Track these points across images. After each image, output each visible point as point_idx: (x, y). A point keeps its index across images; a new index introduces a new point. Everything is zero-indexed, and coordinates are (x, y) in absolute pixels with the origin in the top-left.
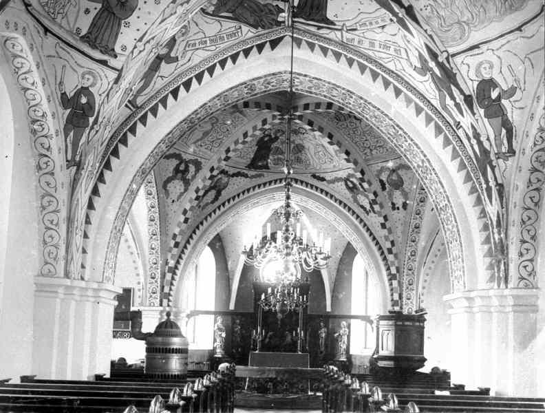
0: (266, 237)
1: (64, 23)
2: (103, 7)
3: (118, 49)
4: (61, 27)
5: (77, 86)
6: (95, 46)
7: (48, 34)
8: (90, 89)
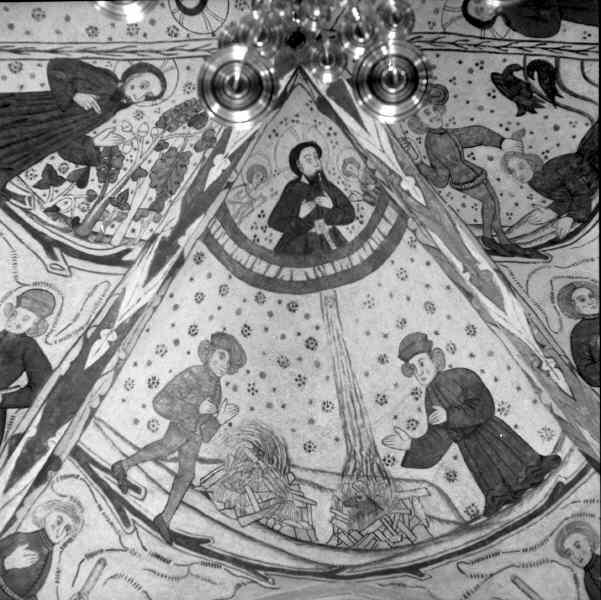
1: (437, 529)
2: (456, 441)
3: (543, 448)
4: (435, 540)
5: (575, 578)
6: (516, 493)
7: (422, 570)
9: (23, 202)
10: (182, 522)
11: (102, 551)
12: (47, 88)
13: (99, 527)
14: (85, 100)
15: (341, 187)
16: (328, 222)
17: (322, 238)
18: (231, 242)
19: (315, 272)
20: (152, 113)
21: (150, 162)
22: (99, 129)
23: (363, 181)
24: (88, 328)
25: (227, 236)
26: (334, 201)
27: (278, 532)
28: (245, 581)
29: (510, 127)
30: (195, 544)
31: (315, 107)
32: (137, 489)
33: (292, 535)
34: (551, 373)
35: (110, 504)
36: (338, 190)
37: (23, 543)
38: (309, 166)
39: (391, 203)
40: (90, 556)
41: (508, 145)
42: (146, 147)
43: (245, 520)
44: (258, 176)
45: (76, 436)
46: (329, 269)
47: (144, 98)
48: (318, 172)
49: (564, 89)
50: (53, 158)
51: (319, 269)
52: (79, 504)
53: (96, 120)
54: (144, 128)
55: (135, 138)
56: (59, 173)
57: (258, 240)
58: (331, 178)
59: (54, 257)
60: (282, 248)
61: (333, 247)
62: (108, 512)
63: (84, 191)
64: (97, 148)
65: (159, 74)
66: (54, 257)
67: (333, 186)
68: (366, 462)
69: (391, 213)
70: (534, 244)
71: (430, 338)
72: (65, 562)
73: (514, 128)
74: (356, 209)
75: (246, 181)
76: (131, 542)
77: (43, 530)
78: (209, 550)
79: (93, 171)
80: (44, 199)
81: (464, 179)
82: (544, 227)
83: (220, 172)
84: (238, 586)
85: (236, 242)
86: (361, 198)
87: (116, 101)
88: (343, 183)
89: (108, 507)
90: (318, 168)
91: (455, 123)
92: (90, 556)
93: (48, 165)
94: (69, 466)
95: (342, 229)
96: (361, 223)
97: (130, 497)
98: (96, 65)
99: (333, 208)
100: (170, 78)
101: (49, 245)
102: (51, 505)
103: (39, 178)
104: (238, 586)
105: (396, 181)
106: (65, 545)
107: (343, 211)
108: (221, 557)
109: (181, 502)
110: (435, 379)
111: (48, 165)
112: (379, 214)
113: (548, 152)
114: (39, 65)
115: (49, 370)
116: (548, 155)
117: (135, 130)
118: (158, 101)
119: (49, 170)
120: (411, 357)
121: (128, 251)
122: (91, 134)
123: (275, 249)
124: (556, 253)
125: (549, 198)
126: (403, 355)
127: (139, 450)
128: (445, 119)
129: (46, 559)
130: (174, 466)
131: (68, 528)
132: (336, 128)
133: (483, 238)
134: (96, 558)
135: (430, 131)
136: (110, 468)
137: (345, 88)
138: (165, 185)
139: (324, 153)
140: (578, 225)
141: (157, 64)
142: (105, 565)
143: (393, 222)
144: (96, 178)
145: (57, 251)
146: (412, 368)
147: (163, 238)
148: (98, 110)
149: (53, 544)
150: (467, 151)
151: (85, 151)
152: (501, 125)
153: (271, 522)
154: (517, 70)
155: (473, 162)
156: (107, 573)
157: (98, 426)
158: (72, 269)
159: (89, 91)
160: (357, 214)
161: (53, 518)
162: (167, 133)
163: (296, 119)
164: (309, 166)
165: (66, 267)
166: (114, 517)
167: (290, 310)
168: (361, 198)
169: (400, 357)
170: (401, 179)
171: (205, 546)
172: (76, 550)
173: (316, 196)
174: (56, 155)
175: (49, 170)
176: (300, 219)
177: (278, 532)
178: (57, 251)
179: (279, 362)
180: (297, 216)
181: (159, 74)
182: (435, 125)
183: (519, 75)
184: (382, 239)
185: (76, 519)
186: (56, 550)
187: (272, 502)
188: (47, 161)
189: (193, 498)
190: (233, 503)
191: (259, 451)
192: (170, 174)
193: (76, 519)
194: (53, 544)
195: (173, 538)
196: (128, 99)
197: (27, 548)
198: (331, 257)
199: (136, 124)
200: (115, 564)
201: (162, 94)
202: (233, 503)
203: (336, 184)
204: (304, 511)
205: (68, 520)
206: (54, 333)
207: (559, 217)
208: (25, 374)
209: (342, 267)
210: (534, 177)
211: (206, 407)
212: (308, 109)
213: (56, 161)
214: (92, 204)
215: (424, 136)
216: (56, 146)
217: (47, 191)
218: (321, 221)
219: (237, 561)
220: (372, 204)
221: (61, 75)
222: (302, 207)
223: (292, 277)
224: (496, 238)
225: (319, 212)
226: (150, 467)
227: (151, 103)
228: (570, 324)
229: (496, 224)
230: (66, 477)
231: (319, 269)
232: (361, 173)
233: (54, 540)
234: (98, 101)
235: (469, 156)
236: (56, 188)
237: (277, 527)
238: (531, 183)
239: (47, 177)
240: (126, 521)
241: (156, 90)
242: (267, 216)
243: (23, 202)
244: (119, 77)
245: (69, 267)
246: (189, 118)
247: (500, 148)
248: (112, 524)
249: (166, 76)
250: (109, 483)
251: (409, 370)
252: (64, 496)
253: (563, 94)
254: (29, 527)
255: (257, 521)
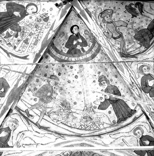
0: (49, 53)
1: (105, 126)
2: (112, 104)
3: (132, 108)
4: (105, 128)
5: (137, 140)
6: (125, 118)
7: (101, 136)
8: (144, 135)
9: (1, 42)
10: (43, 123)
11: (23, 131)
12: (6, 11)
13: (22, 125)
14: (17, 14)
15: (84, 37)
16: (81, 46)
17: (79, 50)
18: (55, 52)
19: (77, 58)
20: (34, 18)
21: (34, 31)
22: (20, 22)
23: (90, 36)
24: (18, 76)
25: (54, 51)
26: (82, 41)
27: (67, 125)
28: (58, 137)
29: (130, 21)
30: (46, 129)
31: (77, 16)
32: (32, 116)
33: (70, 126)
34: (135, 90)
35: (25, 120)
36: (83, 38)
37: (4, 131)
38: (76, 32)
39: (96, 42)
40: (20, 133)
41: (129, 26)
42: (33, 26)
43: (58, 122)
44: (62, 34)
45: (16, 104)
46: (81, 58)
47: (32, 13)
48: (78, 33)
49: (145, 11)
50: (8, 30)
51: (78, 58)
52: (17, 120)
53: (19, 19)
54: (32, 21)
55: (30, 24)
56: (11, 34)
57: (62, 51)
58: (82, 35)
59: (10, 57)
60: (69, 52)
61: (82, 52)
62: (25, 122)
63: (16, 39)
64: (20, 27)
65: (36, 6)
66: (10, 57)
67: (82, 37)
68: (89, 107)
69: (96, 45)
70: (134, 54)
71: (106, 77)
72: (14, 134)
73: (130, 21)
74: (88, 43)
75: (59, 36)
76: (30, 128)
77: (9, 127)
78: (49, 130)
79: (19, 33)
80: (7, 41)
81: (116, 36)
82: (137, 49)
83: (51, 35)
84: (56, 139)
85: (56, 52)
86: (89, 40)
87: (24, 14)
88: (84, 36)
89: (24, 120)
90: (78, 32)
91: (114, 20)
92: (20, 133)
93: (7, 32)
94: (14, 111)
95: (84, 48)
96: (89, 47)
97: (30, 118)
98: (19, 4)
99: (82, 42)
100: (39, 7)
101: (8, 54)
102: (10, 121)
103: (5, 35)
104: (56, 139)
105: (97, 38)
106: (14, 130)
107: (85, 43)
108: (52, 132)
109: (43, 118)
110: (107, 87)
111: (7, 32)
112: (94, 45)
113: (139, 28)
114: (4, 5)
115: (8, 87)
116: (139, 29)
117: (30, 22)
118: (36, 14)
119: (8, 33)
120: (101, 82)
121: (28, 55)
122: (18, 23)
123: (67, 53)
124: (139, 56)
125: (139, 41)
126: (99, 81)
127: (32, 106)
128: (113, 18)
129: (10, 134)
130: (41, 110)
131: (15, 126)
132: (82, 22)
133: (120, 52)
134: (22, 133)
135: (108, 23)
136: (25, 111)
137: (84, 11)
138: (38, 37)
139: (80, 28)
140: (146, 49)
141: (35, 3)
142: (24, 135)
143: (97, 47)
144: (20, 36)
145: (10, 55)
146: (102, 84)
147: (37, 53)
148: (20, 16)
149: (11, 130)
150: (117, 28)
151: (17, 28)
152: (127, 20)
153: (65, 123)
154: (132, 5)
155: (119, 31)
156: (24, 136)
157: (21, 101)
158: (14, 60)
159: (17, 11)
160: (88, 45)
161: (11, 123)
162: (38, 23)
163: (72, 19)
164: (76, 32)
165: (13, 60)
166: (26, 123)
167: (71, 68)
168: (89, 40)
169: (99, 81)
170: (99, 37)
171: (48, 129)
172: (17, 131)
173: (77, 39)
174: (9, 29)
175: (8, 33)
176: (73, 45)
177: (67, 125)
178: (10, 55)
179: (68, 82)
180: (73, 44)
181: (36, 6)
182: (109, 21)
183: (133, 6)
184: (94, 51)
185: (17, 124)
186: (12, 131)
187: (66, 117)
188: (7, 30)
189: (46, 117)
190: (55, 118)
191: (62, 105)
192: (38, 35)
193: (17, 124)
194: (11, 130)
195: (41, 127)
196: (28, 13)
197: (5, 132)
198: (80, 54)
199: (30, 20)
200: (27, 134)
201: (37, 11)
202: (55, 118)
203: (83, 36)
204: (73, 120)
205: (14, 124)
206: (10, 77)
207: (141, 46)
208: (3, 88)
209: (84, 58)
210: (135, 35)
211: (49, 94)
212: (75, 16)
213: (9, 30)
214: (19, 42)
215: (106, 24)
216: (9, 27)
217: (7, 39)
218: (79, 46)
219: (56, 133)
220: (92, 42)
221: (10, 7)
222: (74, 42)
223: (71, 60)
224: (124, 53)
225: (78, 43)
226: (35, 110)
227: (33, 14)
228: (142, 76)
229: (124, 48)
230: (14, 114)
231: (78, 58)
232: (89, 34)
233: (11, 129)
234: (20, 14)
235: (118, 29)
236: (10, 38)
237: (66, 124)
238: (134, 37)
239: (7, 35)
240: (29, 124)
241: (35, 10)
242: (65, 44)
243: (1, 42)
244: (25, 7)
245: (14, 60)
246: (44, 19)
247: (127, 27)
248: (25, 125)
249: (38, 6)
250: (25, 115)
251: (101, 84)
252: (14, 119)
253: (144, 12)
254: (5, 126)
255: (62, 122)
